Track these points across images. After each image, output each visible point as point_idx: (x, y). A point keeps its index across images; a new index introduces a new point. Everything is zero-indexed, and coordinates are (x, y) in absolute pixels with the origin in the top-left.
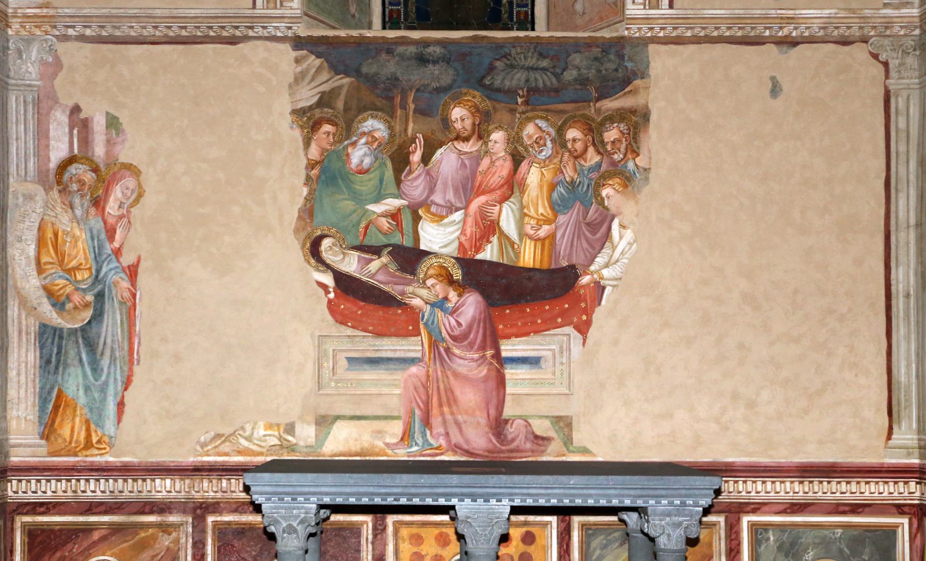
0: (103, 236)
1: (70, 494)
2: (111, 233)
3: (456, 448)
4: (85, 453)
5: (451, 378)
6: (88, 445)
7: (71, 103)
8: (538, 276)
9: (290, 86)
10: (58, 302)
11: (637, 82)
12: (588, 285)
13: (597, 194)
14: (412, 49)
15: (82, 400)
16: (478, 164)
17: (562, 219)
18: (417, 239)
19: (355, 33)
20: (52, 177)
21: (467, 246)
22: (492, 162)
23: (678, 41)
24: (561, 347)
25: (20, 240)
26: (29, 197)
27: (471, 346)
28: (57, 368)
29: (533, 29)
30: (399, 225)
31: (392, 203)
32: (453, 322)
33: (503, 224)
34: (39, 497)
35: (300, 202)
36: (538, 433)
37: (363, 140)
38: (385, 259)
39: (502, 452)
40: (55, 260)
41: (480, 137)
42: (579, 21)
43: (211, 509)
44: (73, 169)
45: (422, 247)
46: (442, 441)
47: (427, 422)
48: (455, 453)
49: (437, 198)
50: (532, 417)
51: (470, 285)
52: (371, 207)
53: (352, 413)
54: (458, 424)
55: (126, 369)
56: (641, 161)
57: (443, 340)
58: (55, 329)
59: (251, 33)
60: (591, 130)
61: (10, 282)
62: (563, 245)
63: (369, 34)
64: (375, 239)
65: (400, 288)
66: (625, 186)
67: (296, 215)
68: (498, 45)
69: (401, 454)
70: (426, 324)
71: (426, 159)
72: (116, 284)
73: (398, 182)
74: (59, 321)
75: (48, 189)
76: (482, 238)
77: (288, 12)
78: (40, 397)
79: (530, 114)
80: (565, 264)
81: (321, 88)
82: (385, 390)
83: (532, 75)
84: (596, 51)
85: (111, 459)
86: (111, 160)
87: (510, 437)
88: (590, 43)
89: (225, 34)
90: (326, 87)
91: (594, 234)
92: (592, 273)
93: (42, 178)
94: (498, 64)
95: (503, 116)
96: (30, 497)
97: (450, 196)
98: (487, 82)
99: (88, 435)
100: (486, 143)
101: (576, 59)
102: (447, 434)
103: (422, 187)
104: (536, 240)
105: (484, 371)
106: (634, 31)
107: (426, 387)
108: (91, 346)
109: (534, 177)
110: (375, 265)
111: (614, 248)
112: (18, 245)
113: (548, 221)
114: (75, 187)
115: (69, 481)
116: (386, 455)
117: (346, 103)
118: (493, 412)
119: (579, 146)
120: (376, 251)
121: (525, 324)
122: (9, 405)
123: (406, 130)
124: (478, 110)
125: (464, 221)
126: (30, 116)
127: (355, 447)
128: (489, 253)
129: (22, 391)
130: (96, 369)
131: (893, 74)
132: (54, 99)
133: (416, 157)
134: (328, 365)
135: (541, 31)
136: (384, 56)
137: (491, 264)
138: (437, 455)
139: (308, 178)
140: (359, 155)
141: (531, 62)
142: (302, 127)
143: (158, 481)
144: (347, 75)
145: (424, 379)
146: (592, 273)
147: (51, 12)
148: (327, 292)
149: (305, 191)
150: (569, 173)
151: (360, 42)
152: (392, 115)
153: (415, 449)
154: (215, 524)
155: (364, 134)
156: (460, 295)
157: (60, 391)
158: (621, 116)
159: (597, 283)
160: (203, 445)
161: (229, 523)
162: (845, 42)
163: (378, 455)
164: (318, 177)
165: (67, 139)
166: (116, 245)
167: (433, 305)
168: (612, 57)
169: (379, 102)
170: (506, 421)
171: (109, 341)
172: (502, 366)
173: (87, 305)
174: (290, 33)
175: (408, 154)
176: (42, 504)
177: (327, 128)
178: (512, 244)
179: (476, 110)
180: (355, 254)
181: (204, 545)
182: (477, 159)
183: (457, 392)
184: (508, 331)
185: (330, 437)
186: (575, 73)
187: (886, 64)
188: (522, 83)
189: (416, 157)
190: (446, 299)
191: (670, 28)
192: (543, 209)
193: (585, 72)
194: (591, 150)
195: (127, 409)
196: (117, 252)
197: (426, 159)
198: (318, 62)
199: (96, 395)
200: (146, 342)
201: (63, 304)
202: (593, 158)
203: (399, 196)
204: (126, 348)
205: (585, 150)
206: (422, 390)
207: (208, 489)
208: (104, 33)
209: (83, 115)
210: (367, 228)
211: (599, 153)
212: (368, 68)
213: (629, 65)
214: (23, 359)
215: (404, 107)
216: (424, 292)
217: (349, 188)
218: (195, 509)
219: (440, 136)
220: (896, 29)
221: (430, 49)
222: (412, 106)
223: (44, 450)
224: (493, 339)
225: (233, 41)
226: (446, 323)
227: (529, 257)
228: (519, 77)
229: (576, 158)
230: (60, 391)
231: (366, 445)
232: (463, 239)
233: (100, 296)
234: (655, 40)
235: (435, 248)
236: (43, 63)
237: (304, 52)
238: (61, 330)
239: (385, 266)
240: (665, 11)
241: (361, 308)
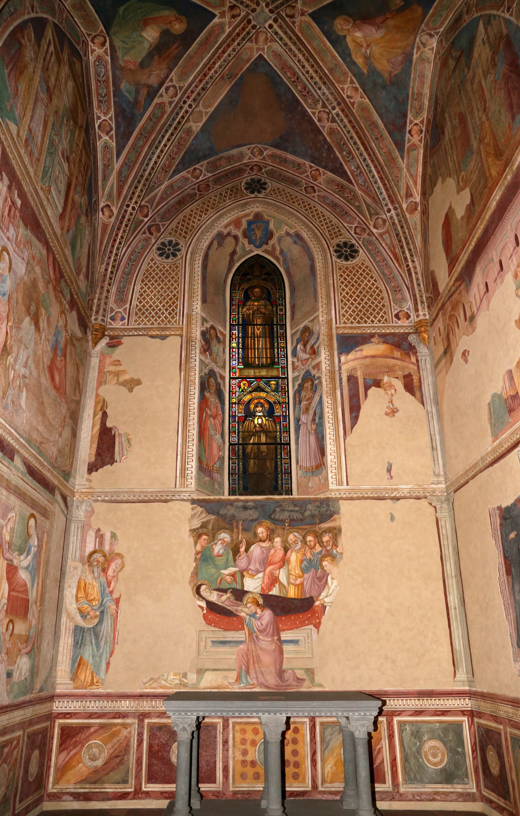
0: (106, 585)
1: (82, 708)
2: (109, 584)
3: (261, 685)
4: (90, 687)
5: (259, 651)
7: (97, 528)
8: (296, 602)
9: (189, 520)
10: (84, 615)
11: (335, 516)
12: (318, 606)
13: (321, 565)
14: (241, 504)
15: (91, 661)
16: (269, 552)
17: (306, 576)
18: (243, 585)
19: (217, 497)
20: (86, 559)
21: (265, 588)
22: (276, 551)
23: (352, 499)
24: (308, 635)
25: (70, 587)
26: (75, 568)
27: (267, 635)
28: (81, 646)
29: (292, 495)
30: (235, 579)
31: (232, 570)
32: (259, 624)
33: (280, 578)
35: (192, 569)
36: (299, 677)
37: (220, 542)
38: (229, 595)
39: (282, 686)
40: (84, 596)
41: (270, 540)
42: (310, 491)
43: (147, 716)
44: (95, 556)
45: (245, 589)
46: (255, 681)
47: (248, 672)
48: (261, 687)
49: (252, 567)
50: (296, 669)
51: (267, 606)
52: (223, 571)
53: (213, 667)
54: (262, 674)
55: (111, 646)
56: (339, 549)
57: (255, 632)
58: (81, 628)
59: (174, 498)
60: (317, 536)
61: (64, 606)
62: (307, 587)
63: (223, 498)
64: (224, 586)
65: (235, 608)
66: (333, 561)
67: (190, 575)
68: (277, 502)
69: (236, 689)
70: (247, 625)
71: (247, 550)
72: (109, 607)
73: (235, 560)
74: (84, 624)
75: (84, 564)
76: (271, 584)
77: (189, 489)
78: (72, 660)
79: (291, 530)
80: (308, 596)
81: (202, 520)
82: (228, 656)
83: (292, 514)
84: (318, 503)
85: (102, 691)
86: (112, 552)
87: (286, 679)
88: (315, 500)
89: (163, 498)
90: (204, 520)
91: (320, 582)
92: (320, 600)
93: (82, 560)
94: (277, 509)
95: (279, 531)
97: (257, 566)
98: (273, 517)
100: (273, 543)
101: (310, 507)
102: (257, 677)
103: (245, 563)
104: (295, 585)
105: (273, 647)
106: (333, 495)
107: (247, 655)
108: (97, 636)
109: (293, 557)
110: (225, 597)
111: (329, 589)
112: (69, 589)
113: (300, 577)
114: (95, 563)
115: (82, 701)
116: (229, 688)
117: (213, 526)
118: (278, 666)
119: (312, 543)
120: (225, 591)
121: (291, 624)
122: (58, 664)
123: (238, 538)
124: (269, 528)
125: (264, 577)
126: (79, 533)
127: (214, 684)
128: (275, 591)
129: (64, 658)
131: (438, 511)
132: (90, 526)
133: (242, 549)
134: (203, 644)
135: (295, 495)
136: (229, 507)
137: (276, 597)
138: (252, 688)
139: (196, 559)
140: (218, 549)
141: (291, 508)
142: (194, 537)
143: (123, 702)
144: (213, 514)
145: (246, 651)
146: (320, 600)
147: (92, 491)
148: (203, 610)
149: (194, 564)
150: (309, 555)
151: (219, 501)
152: (232, 531)
153: (242, 685)
154: (149, 724)
155: (220, 539)
156: (262, 611)
157: (81, 657)
158: (329, 530)
159: (323, 605)
160: (145, 684)
161: (155, 723)
162: (418, 498)
163: (225, 688)
164: (200, 558)
165: (93, 543)
166: (111, 589)
167: (250, 616)
168: (324, 506)
169: (227, 526)
170: (284, 671)
171: (105, 633)
172: (281, 644)
173: (96, 617)
174: (190, 498)
175: (239, 548)
177: (204, 537)
178: (285, 587)
179: (268, 529)
180: (216, 592)
181: (143, 734)
182: (269, 549)
183: (262, 657)
184: (284, 628)
185: (203, 680)
186: (309, 512)
187: (435, 507)
188: (287, 517)
189: (242, 549)
190: (256, 613)
191: (347, 494)
192: (298, 572)
193: (313, 512)
194: (317, 545)
196: (111, 592)
197: (247, 550)
198: (201, 509)
199: (97, 659)
201: (86, 616)
202: (318, 548)
204: (112, 636)
205: (315, 545)
206: (245, 656)
207: (146, 706)
208: (113, 499)
209: (101, 533)
210: (221, 581)
211: (321, 546)
212: (222, 512)
213: (332, 509)
214: (66, 641)
215: (237, 527)
216: (246, 610)
217: (213, 562)
218: (139, 716)
219: (253, 540)
220: (437, 493)
221: (249, 504)
222: (241, 527)
224: (277, 631)
225: (166, 501)
226: (256, 624)
227: (292, 593)
228: (286, 515)
229: (311, 549)
230: (81, 657)
231: (220, 683)
232: (263, 585)
233: (102, 612)
234: (342, 498)
235: (251, 589)
236: (87, 511)
237: (196, 505)
238: (84, 628)
239: (228, 598)
240: (345, 486)
241: (218, 617)
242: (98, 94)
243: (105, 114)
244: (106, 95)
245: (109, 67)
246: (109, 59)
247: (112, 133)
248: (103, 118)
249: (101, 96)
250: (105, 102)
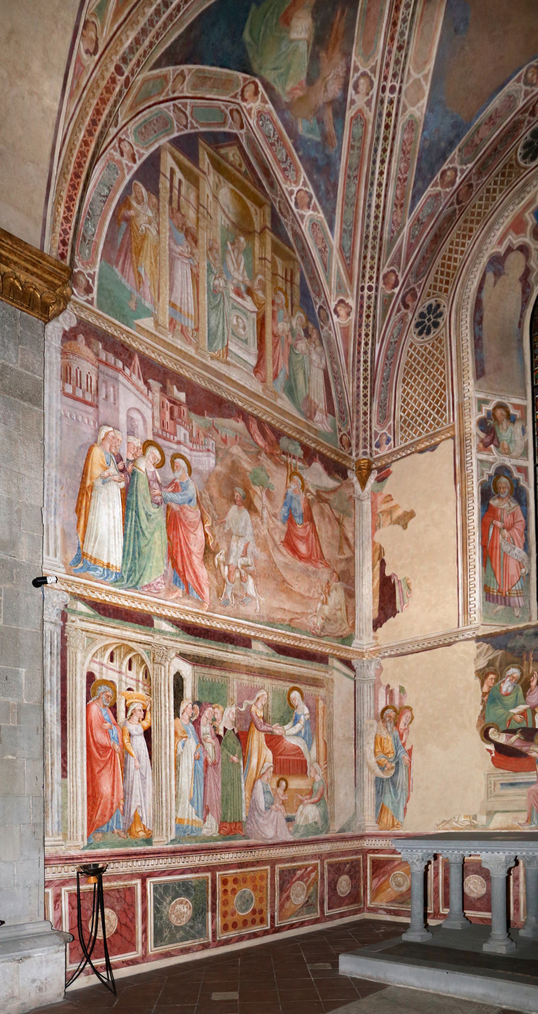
6: (393, 826)
15: (391, 807)
34: (376, 847)
67: (477, 719)
96: (373, 847)
99: (393, 822)
130: (396, 794)
176: (377, 850)
195: (408, 811)
200: (415, 783)
203: (525, 703)
223: (377, 828)
230: (383, 804)
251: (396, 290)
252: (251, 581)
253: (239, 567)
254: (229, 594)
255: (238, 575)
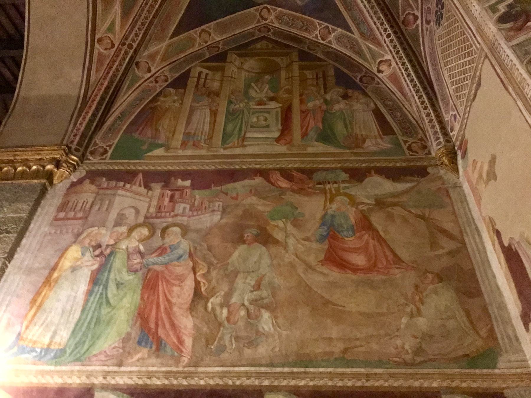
242: (301, 29)
243: (316, 29)
244: (302, 22)
245: (284, 11)
246: (279, 9)
247: (330, 29)
248: (318, 32)
249: (303, 26)
250: (307, 25)
251: (419, 22)
252: (266, 315)
253: (246, 303)
254: (227, 338)
255: (243, 313)
